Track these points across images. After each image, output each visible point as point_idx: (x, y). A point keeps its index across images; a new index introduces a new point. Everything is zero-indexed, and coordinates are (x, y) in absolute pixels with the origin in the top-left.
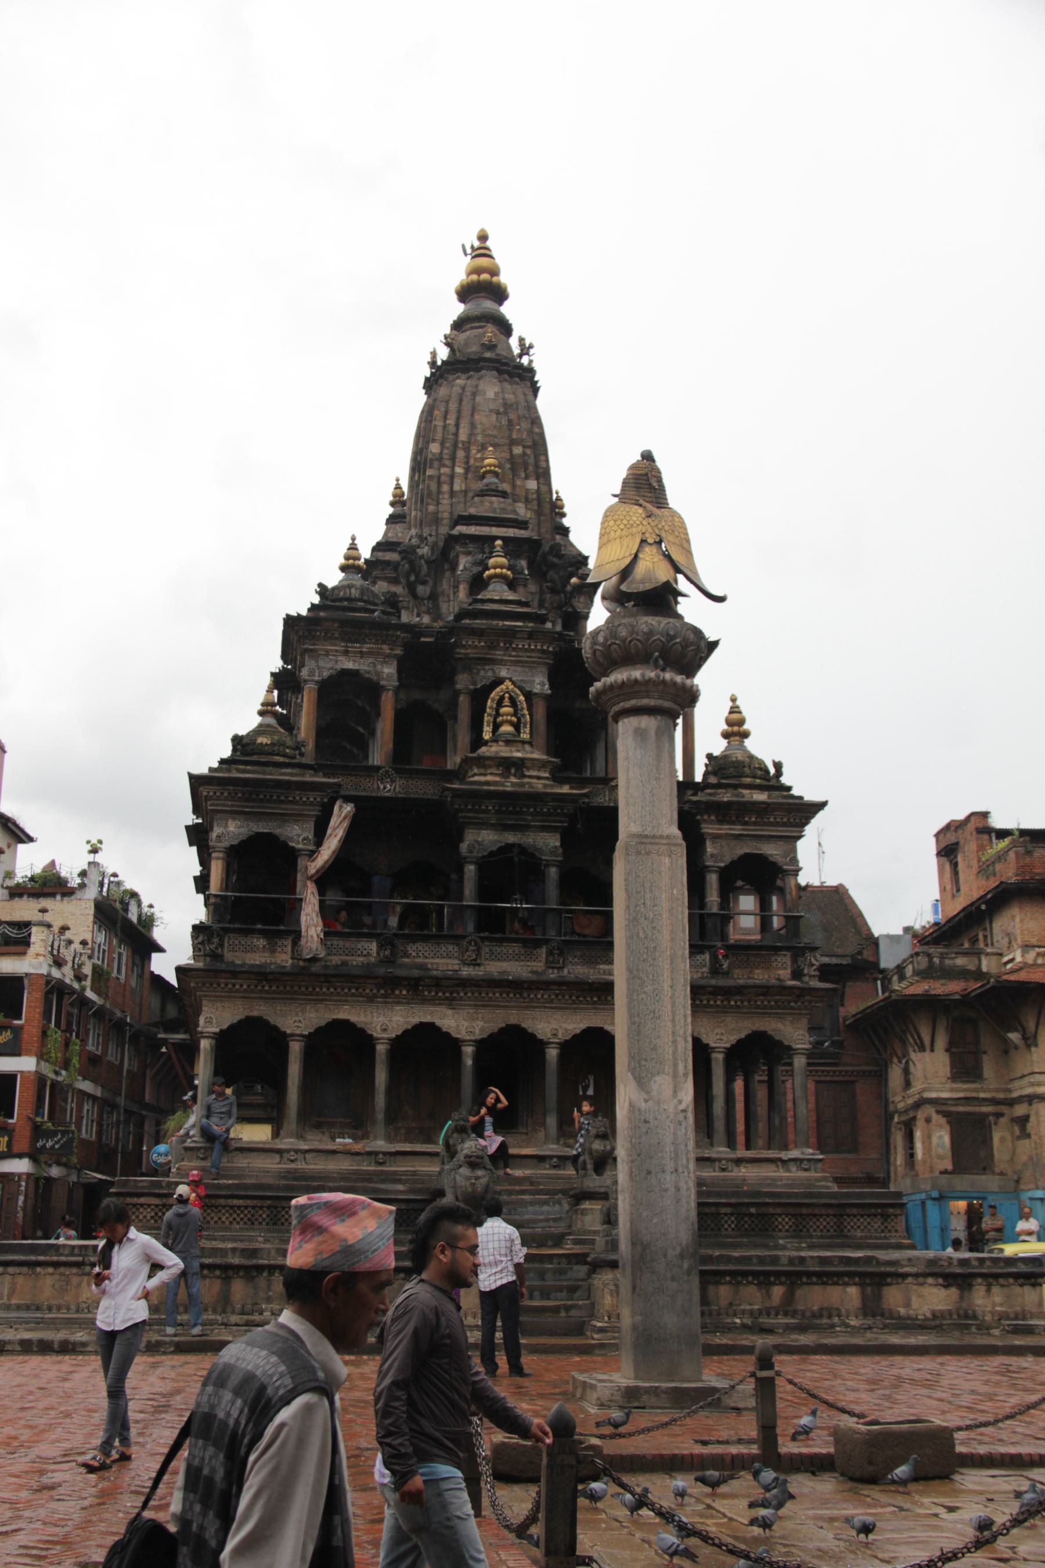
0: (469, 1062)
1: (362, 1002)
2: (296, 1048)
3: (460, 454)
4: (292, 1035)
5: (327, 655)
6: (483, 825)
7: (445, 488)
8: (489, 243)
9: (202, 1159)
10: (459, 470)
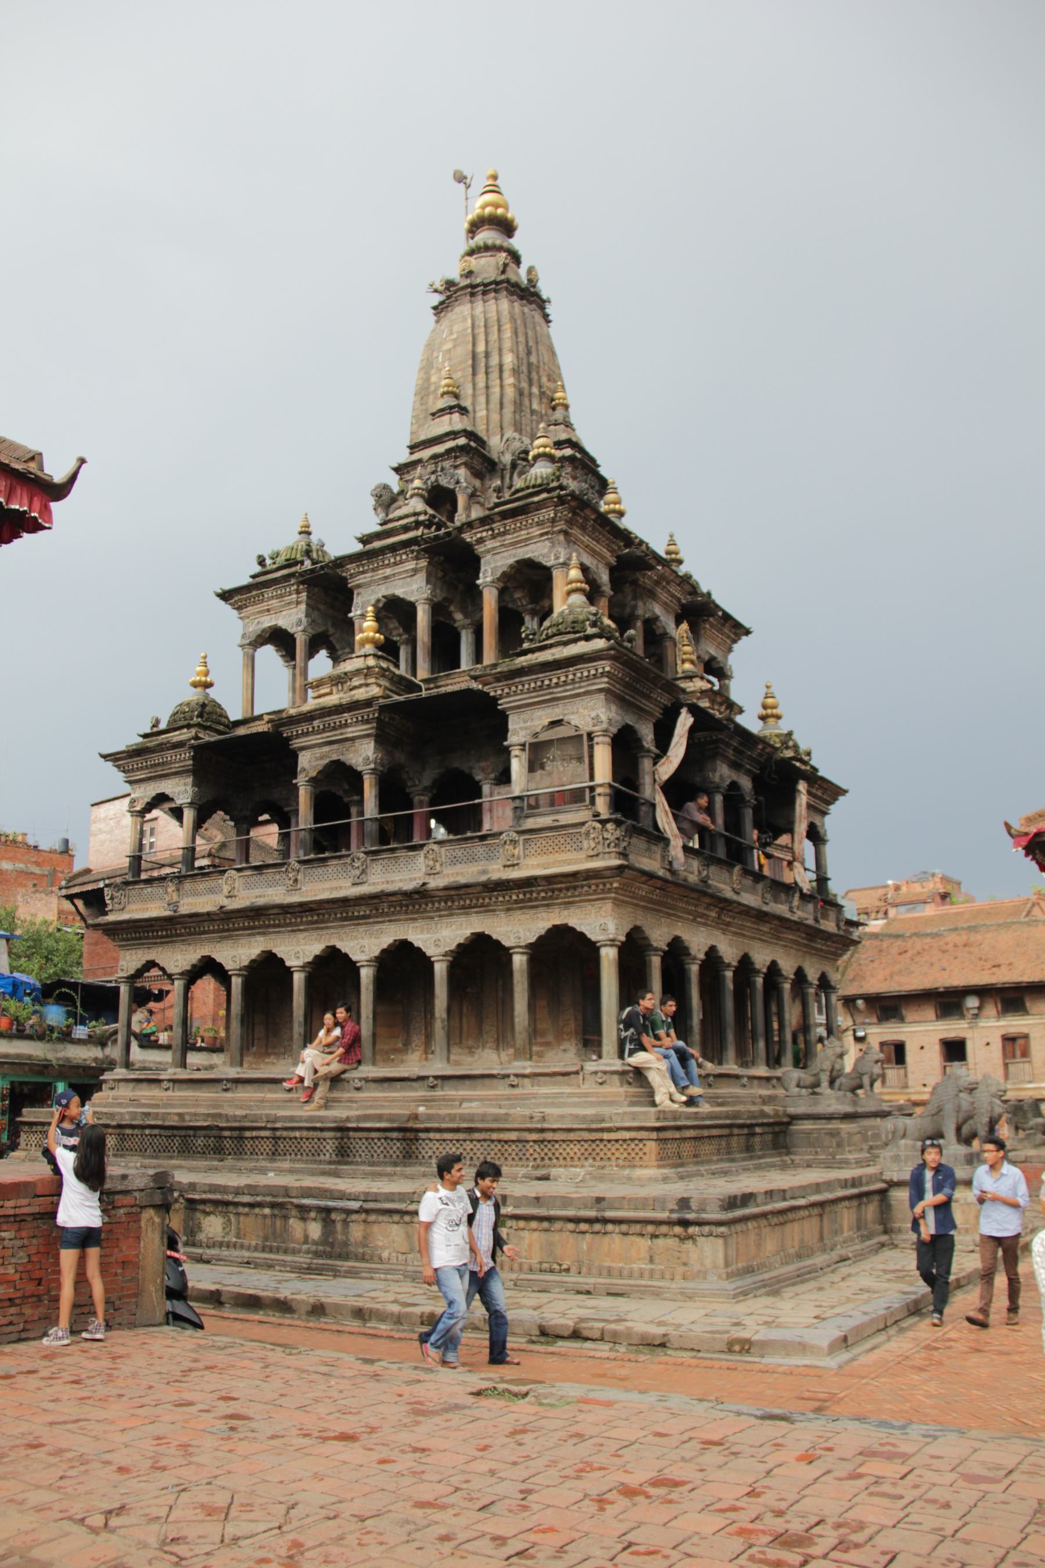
0: (730, 985)
1: (687, 919)
2: (656, 961)
3: (534, 376)
4: (656, 949)
5: (575, 543)
6: (725, 759)
7: (526, 402)
8: (498, 182)
9: (630, 1084)
10: (535, 390)
